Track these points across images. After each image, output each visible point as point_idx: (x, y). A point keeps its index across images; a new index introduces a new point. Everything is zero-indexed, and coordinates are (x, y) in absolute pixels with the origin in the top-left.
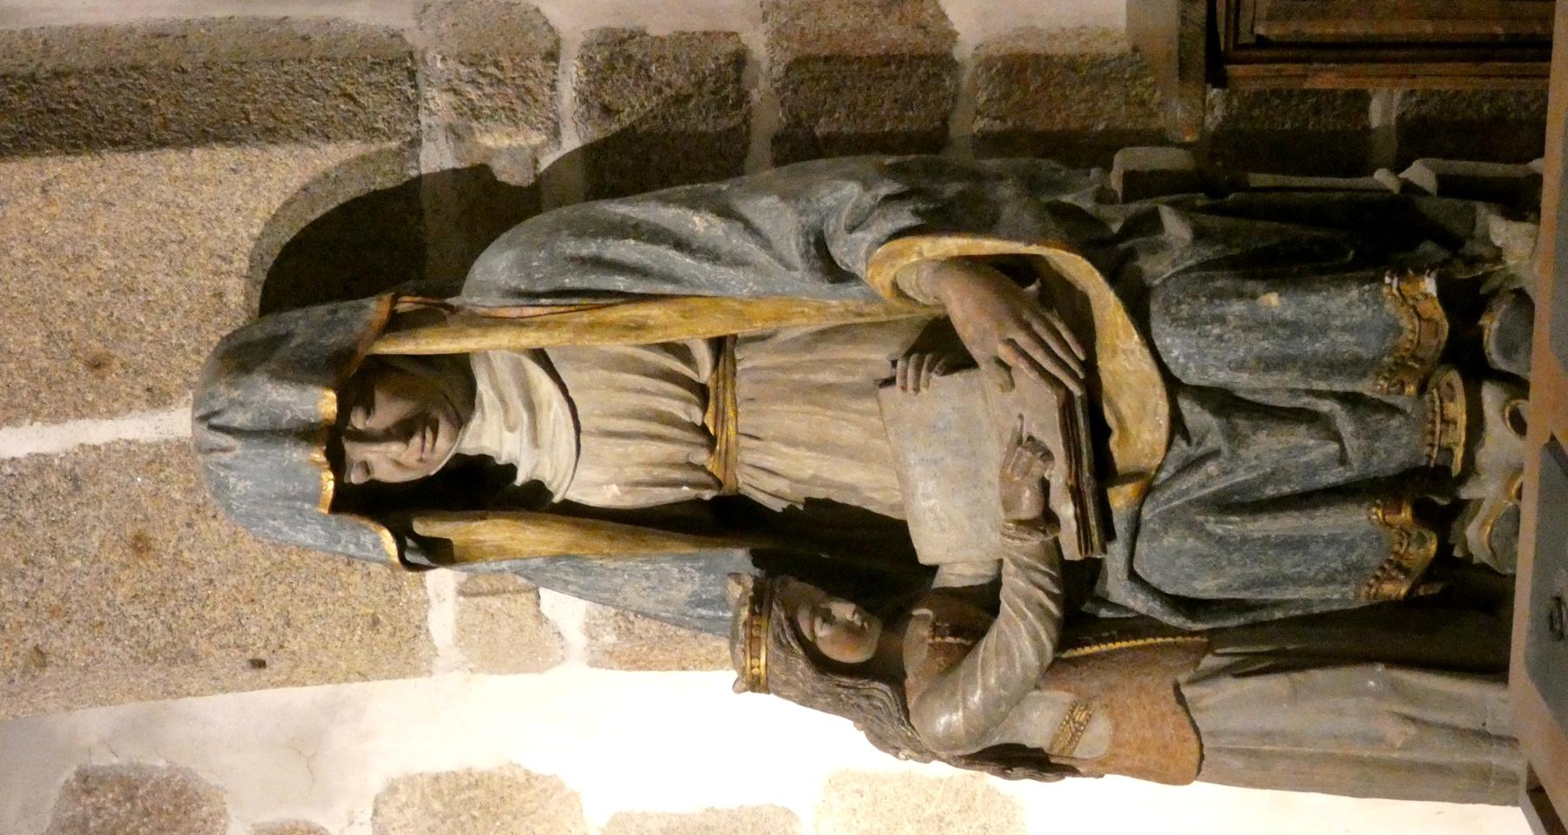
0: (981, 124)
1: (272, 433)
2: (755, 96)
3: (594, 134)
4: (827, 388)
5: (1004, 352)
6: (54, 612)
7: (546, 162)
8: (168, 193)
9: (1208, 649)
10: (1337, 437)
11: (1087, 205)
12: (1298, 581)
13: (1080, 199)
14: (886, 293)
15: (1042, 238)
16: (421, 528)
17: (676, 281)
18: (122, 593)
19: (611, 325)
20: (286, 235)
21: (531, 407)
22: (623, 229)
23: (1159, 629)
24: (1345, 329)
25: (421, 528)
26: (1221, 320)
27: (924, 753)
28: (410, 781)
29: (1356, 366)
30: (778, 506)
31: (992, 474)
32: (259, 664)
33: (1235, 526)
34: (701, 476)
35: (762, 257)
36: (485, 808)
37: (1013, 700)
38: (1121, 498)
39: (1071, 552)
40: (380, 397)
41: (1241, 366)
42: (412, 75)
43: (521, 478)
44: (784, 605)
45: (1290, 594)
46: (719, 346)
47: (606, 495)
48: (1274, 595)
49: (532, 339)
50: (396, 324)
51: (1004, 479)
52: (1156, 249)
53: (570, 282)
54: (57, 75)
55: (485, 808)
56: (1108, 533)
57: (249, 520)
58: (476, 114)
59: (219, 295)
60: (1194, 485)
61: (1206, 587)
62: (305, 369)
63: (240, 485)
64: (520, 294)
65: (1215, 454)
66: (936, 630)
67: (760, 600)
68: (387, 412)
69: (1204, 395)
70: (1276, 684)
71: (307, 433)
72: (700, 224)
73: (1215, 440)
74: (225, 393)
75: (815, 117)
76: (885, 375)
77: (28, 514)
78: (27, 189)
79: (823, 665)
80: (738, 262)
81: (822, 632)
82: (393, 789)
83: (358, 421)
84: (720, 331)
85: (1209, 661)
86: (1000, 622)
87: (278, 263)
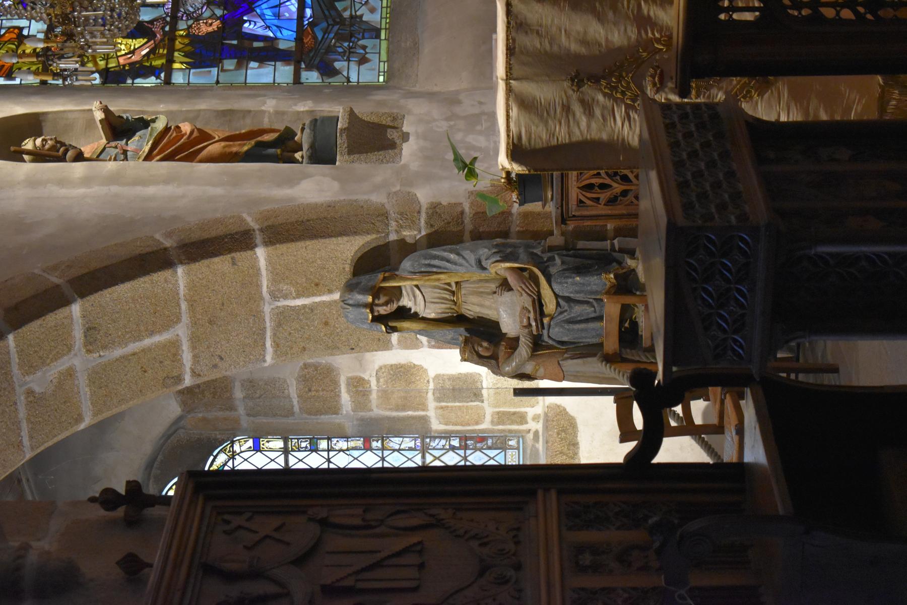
0: (518, 229)
1: (358, 305)
2: (466, 221)
3: (429, 231)
4: (482, 292)
5: (519, 289)
6: (307, 339)
7: (418, 237)
8: (333, 247)
9: (565, 353)
10: (594, 307)
11: (539, 253)
12: (586, 338)
13: (538, 251)
14: (494, 274)
15: (528, 263)
16: (390, 324)
17: (447, 269)
18: (322, 334)
19: (432, 279)
20: (359, 255)
21: (415, 297)
23: (556, 348)
24: (595, 284)
25: (390, 324)
26: (567, 283)
27: (503, 376)
28: (385, 366)
29: (596, 292)
30: (471, 317)
31: (518, 314)
32: (353, 349)
33: (572, 326)
34: (453, 311)
35: (466, 264)
36: (404, 373)
37: (523, 364)
39: (535, 333)
40: (381, 296)
41: (571, 293)
42: (387, 218)
43: (412, 311)
44: (471, 343)
45: (584, 340)
46: (457, 283)
47: (433, 316)
48: (581, 341)
49: (415, 283)
50: (385, 279)
51: (520, 317)
52: (554, 265)
53: (423, 270)
54: (308, 221)
55: (404, 373)
56: (543, 328)
57: (352, 323)
58: (402, 227)
59: (344, 268)
60: (561, 317)
61: (565, 339)
62: (364, 291)
64: (412, 272)
65: (566, 311)
66: (506, 348)
67: (466, 341)
68: (383, 299)
69: (564, 298)
70: (579, 361)
71: (366, 305)
72: (452, 256)
73: (566, 308)
74: (347, 296)
75: (480, 226)
76: (494, 290)
77: (302, 318)
78: (302, 248)
79: (480, 357)
80: (461, 265)
81: (480, 349)
82: (381, 368)
83: (377, 302)
84: (457, 280)
85: (566, 355)
86: (519, 348)
87: (357, 261)
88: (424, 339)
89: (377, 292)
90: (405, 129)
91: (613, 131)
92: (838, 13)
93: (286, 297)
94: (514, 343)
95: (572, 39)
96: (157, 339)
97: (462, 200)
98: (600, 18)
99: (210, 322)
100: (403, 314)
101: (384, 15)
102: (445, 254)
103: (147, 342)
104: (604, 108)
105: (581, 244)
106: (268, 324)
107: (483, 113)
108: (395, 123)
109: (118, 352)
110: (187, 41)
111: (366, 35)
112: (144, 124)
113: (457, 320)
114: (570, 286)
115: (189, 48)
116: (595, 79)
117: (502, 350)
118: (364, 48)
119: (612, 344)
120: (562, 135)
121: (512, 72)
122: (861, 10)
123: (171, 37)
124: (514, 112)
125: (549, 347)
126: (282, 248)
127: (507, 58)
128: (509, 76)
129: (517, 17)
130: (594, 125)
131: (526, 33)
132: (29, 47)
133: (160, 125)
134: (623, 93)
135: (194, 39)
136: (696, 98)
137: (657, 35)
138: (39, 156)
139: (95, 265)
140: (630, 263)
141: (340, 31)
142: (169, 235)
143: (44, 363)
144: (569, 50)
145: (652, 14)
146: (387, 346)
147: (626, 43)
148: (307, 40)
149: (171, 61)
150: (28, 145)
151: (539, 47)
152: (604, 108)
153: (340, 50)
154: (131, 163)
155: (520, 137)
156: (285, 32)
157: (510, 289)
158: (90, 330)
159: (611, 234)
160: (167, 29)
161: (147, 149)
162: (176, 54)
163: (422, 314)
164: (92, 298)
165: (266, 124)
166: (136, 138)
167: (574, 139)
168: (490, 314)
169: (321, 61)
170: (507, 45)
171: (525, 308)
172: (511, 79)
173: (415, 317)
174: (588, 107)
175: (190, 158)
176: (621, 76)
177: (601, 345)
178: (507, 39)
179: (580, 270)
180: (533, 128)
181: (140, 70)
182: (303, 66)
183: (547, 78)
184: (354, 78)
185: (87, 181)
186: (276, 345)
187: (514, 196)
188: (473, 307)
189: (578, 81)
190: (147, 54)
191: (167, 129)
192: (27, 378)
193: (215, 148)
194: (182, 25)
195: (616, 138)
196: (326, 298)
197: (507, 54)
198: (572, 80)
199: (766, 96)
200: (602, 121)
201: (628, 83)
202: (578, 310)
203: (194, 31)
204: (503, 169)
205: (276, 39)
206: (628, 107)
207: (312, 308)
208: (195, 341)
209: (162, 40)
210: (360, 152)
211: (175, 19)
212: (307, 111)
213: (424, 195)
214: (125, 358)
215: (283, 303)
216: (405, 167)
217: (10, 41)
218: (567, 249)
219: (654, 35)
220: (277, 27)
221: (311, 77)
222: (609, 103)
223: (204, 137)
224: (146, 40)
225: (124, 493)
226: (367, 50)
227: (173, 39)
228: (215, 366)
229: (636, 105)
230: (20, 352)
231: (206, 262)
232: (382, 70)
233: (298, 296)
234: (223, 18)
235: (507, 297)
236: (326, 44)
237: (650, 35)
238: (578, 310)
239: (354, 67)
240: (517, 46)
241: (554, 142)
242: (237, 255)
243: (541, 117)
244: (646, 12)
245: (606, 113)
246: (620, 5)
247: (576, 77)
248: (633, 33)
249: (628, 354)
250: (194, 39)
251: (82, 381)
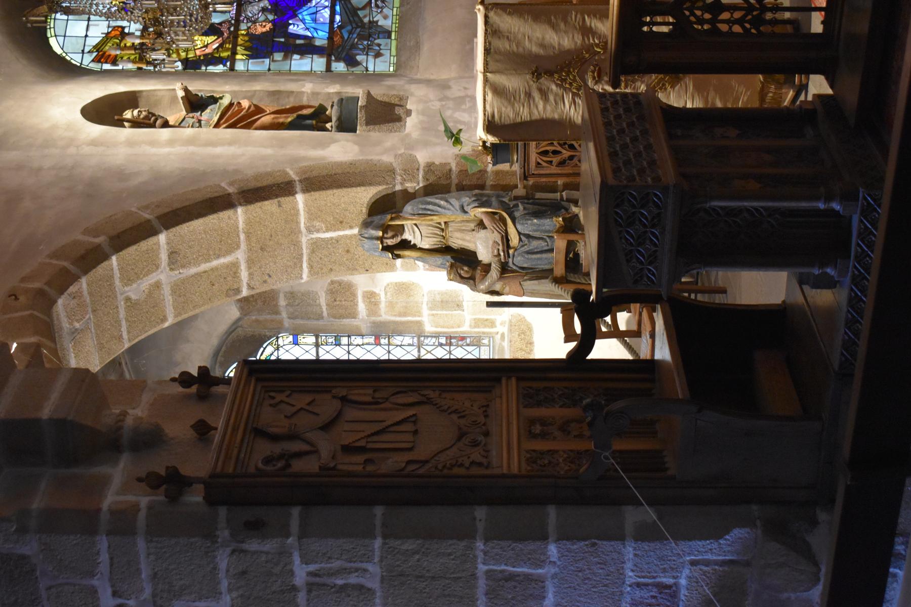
0: (491, 183)
2: (453, 177)
3: (425, 184)
4: (464, 230)
5: (492, 228)
6: (334, 262)
7: (417, 188)
8: (353, 194)
9: (525, 276)
10: (547, 242)
11: (507, 201)
12: (540, 265)
13: (506, 200)
14: (473, 216)
15: (499, 209)
16: (395, 252)
17: (438, 212)
18: (345, 259)
19: (426, 220)
20: (373, 200)
21: (414, 232)
22: (429, 203)
23: (518, 272)
24: (548, 225)
25: (395, 252)
26: (527, 224)
27: (479, 292)
28: (391, 283)
29: (549, 231)
30: (456, 248)
31: (490, 246)
32: (367, 270)
33: (530, 256)
34: (441, 243)
35: (452, 209)
36: (405, 289)
37: (494, 283)
38: (511, 251)
39: (503, 260)
40: (389, 231)
41: (530, 231)
42: (394, 173)
43: (412, 243)
44: (455, 267)
45: (539, 267)
46: (445, 223)
47: (427, 247)
48: (537, 267)
49: (414, 222)
50: (392, 219)
51: (492, 249)
52: (518, 210)
53: (420, 212)
54: (335, 174)
55: (405, 289)
56: (509, 257)
57: (367, 251)
58: (405, 180)
59: (361, 210)
60: (523, 249)
61: (525, 265)
62: (377, 228)
63: (366, 246)
64: (412, 214)
65: (526, 244)
66: (481, 272)
67: (452, 266)
68: (390, 234)
69: (525, 235)
70: (536, 282)
71: (377, 238)
72: (442, 203)
73: (526, 242)
74: (364, 231)
75: (463, 181)
76: (473, 228)
77: (330, 246)
78: (330, 195)
79: (462, 277)
80: (449, 209)
81: (462, 272)
82: (388, 285)
83: (385, 236)
84: (445, 221)
85: (525, 278)
86: (491, 272)
87: (371, 205)
88: (420, 264)
89: (385, 229)
90: (408, 107)
91: (563, 112)
92: (730, 28)
93: (318, 231)
94: (487, 268)
95: (533, 43)
96: (223, 261)
97: (450, 161)
98: (554, 27)
99: (262, 249)
100: (406, 245)
101: (394, 21)
102: (437, 201)
103: (215, 263)
104: (556, 95)
105: (538, 195)
106: (305, 251)
107: (467, 96)
108: (401, 102)
109: (193, 270)
110: (246, 38)
112: (214, 100)
113: (445, 250)
114: (531, 226)
115: (248, 44)
116: (550, 73)
117: (478, 273)
118: (379, 45)
119: (560, 270)
120: (525, 114)
121: (488, 67)
122: (748, 26)
123: (235, 35)
124: (489, 97)
125: (513, 271)
126: (316, 195)
127: (485, 56)
128: (486, 70)
129: (492, 26)
130: (548, 108)
131: (499, 38)
132: (129, 42)
133: (226, 102)
134: (571, 84)
135: (251, 37)
136: (625, 89)
137: (597, 41)
138: (136, 124)
139: (177, 205)
140: (575, 210)
141: (361, 33)
142: (231, 184)
143: (138, 278)
144: (531, 51)
145: (593, 25)
146: (392, 268)
147: (573, 47)
149: (234, 53)
150: (128, 114)
151: (508, 48)
152: (556, 95)
153: (361, 47)
154: (204, 130)
155: (493, 116)
156: (320, 33)
157: (485, 228)
158: (172, 254)
159: (561, 188)
160: (232, 29)
161: (216, 119)
162: (239, 48)
163: (419, 245)
164: (174, 230)
165: (305, 101)
166: (208, 111)
167: (533, 118)
168: (470, 246)
169: (347, 54)
170: (485, 46)
171: (495, 242)
172: (487, 72)
173: (414, 247)
174: (544, 94)
175: (248, 126)
176: (569, 71)
177: (551, 270)
178: (485, 43)
179: (537, 214)
180: (503, 109)
181: (211, 60)
182: (333, 58)
183: (514, 72)
184: (371, 68)
185: (171, 142)
186: (311, 267)
187: (489, 159)
188: (458, 240)
189: (537, 74)
190: (217, 48)
191: (231, 105)
192: (126, 289)
193: (266, 119)
194: (243, 26)
195: (564, 117)
196: (348, 232)
197: (484, 53)
198: (533, 74)
199: (677, 88)
200: (554, 104)
201: (574, 77)
202: (535, 244)
203: (252, 31)
204: (481, 139)
205: (313, 37)
206: (574, 94)
207: (337, 240)
208: (250, 262)
209: (228, 37)
210: (375, 124)
211: (238, 22)
212: (336, 93)
213: (422, 157)
214: (198, 275)
215: (316, 235)
216: (408, 135)
217: (115, 37)
218: (528, 198)
219: (594, 41)
220: (315, 29)
221: (339, 67)
222: (560, 91)
223: (258, 110)
224: (216, 37)
225: (196, 375)
226: (381, 47)
227: (236, 37)
228: (265, 282)
229: (580, 93)
230: (121, 269)
231: (259, 204)
232: (392, 62)
233: (327, 230)
235: (482, 233)
237: (591, 41)
238: (535, 244)
239: (371, 59)
240: (492, 47)
241: (519, 120)
242: (282, 199)
243: (509, 101)
244: (588, 24)
245: (558, 99)
246: (569, 18)
247: (536, 71)
248: (578, 39)
249: (572, 277)
250: (251, 37)
251: (166, 291)
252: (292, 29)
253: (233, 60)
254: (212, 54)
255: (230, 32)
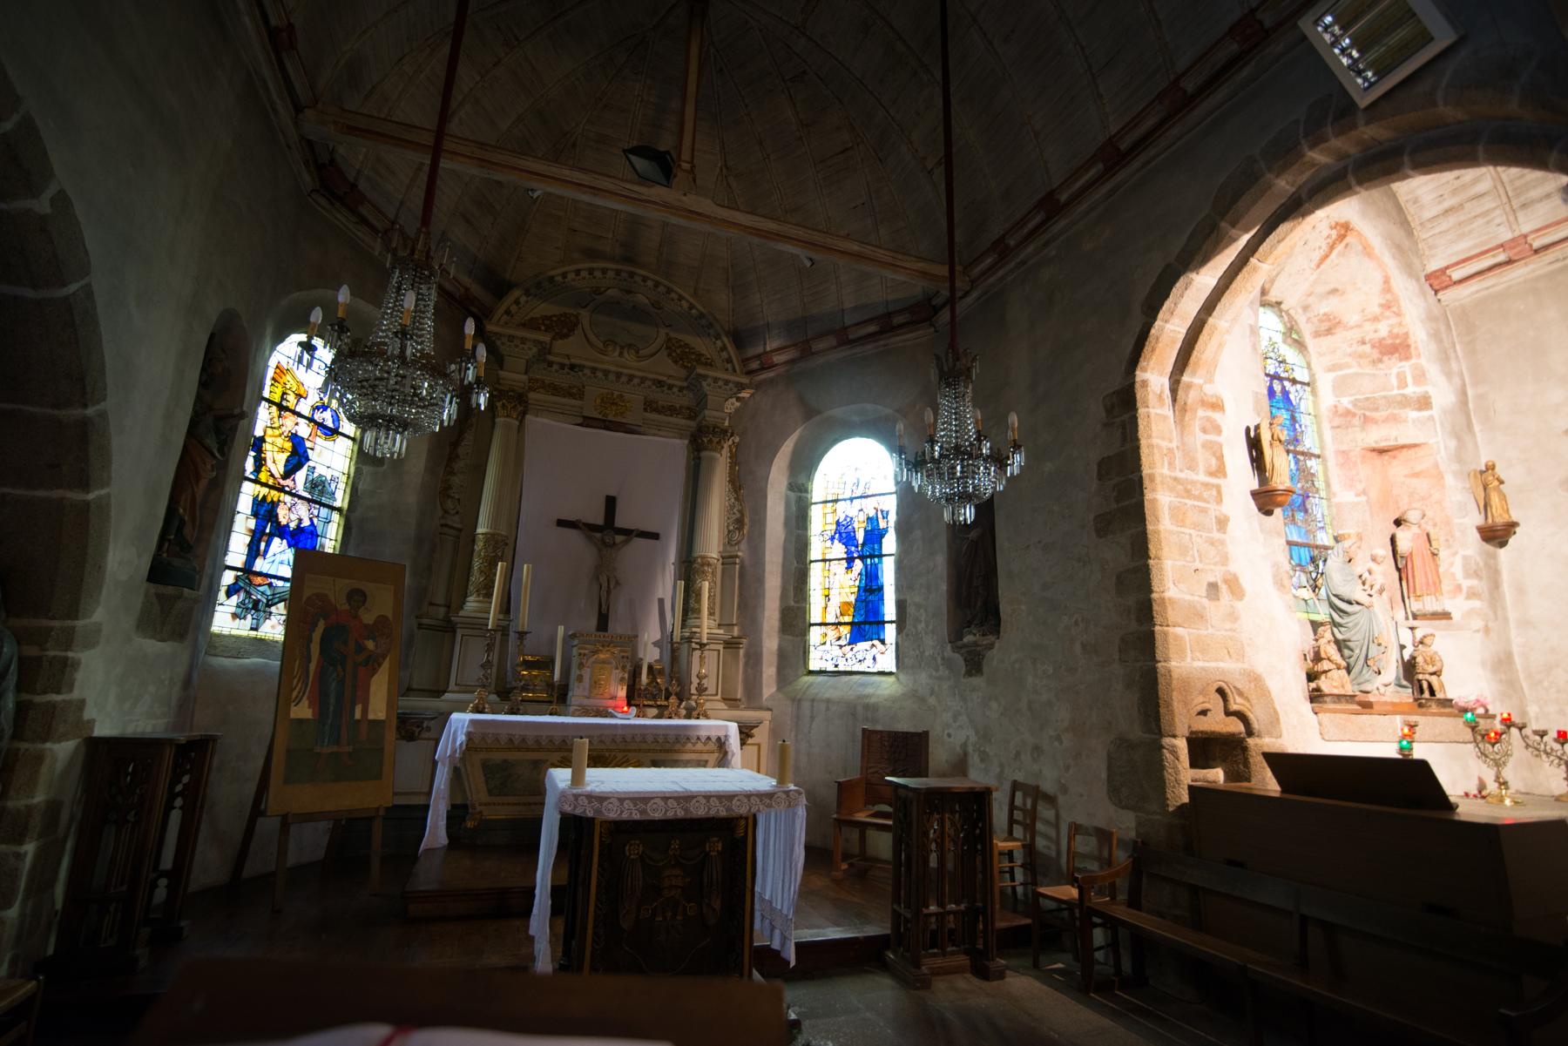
101: (268, 635)
111: (255, 621)
115: (269, 500)
118: (245, 618)
123: (281, 489)
132: (291, 398)
135: (275, 505)
148: (259, 580)
153: (247, 601)
160: (287, 489)
169: (242, 588)
182: (239, 573)
194: (288, 499)
203: (282, 505)
209: (279, 484)
220: (273, 561)
224: (282, 473)
232: (224, 629)
234: (287, 526)
236: (253, 592)
239: (233, 610)
252: (276, 541)
253: (256, 481)
254: (265, 465)
255: (283, 486)
